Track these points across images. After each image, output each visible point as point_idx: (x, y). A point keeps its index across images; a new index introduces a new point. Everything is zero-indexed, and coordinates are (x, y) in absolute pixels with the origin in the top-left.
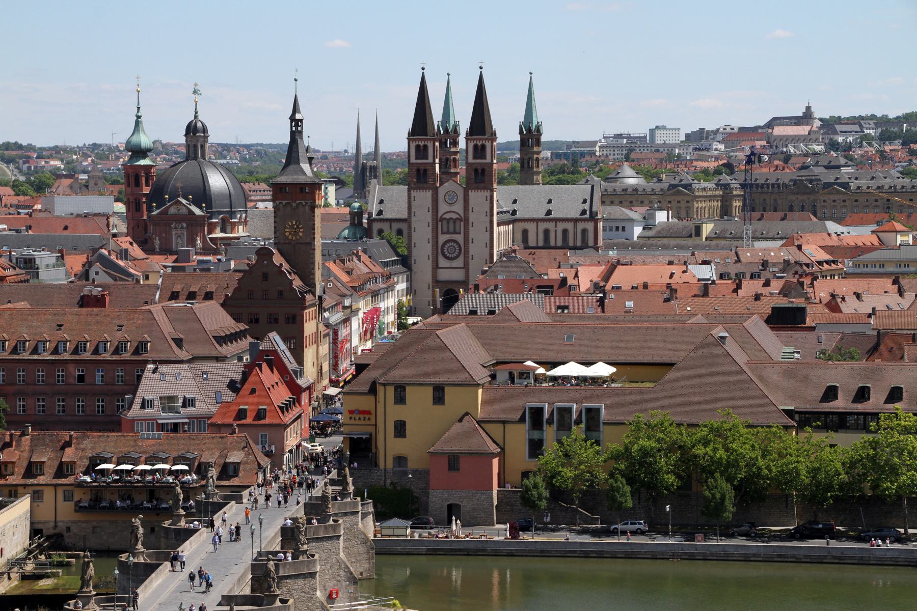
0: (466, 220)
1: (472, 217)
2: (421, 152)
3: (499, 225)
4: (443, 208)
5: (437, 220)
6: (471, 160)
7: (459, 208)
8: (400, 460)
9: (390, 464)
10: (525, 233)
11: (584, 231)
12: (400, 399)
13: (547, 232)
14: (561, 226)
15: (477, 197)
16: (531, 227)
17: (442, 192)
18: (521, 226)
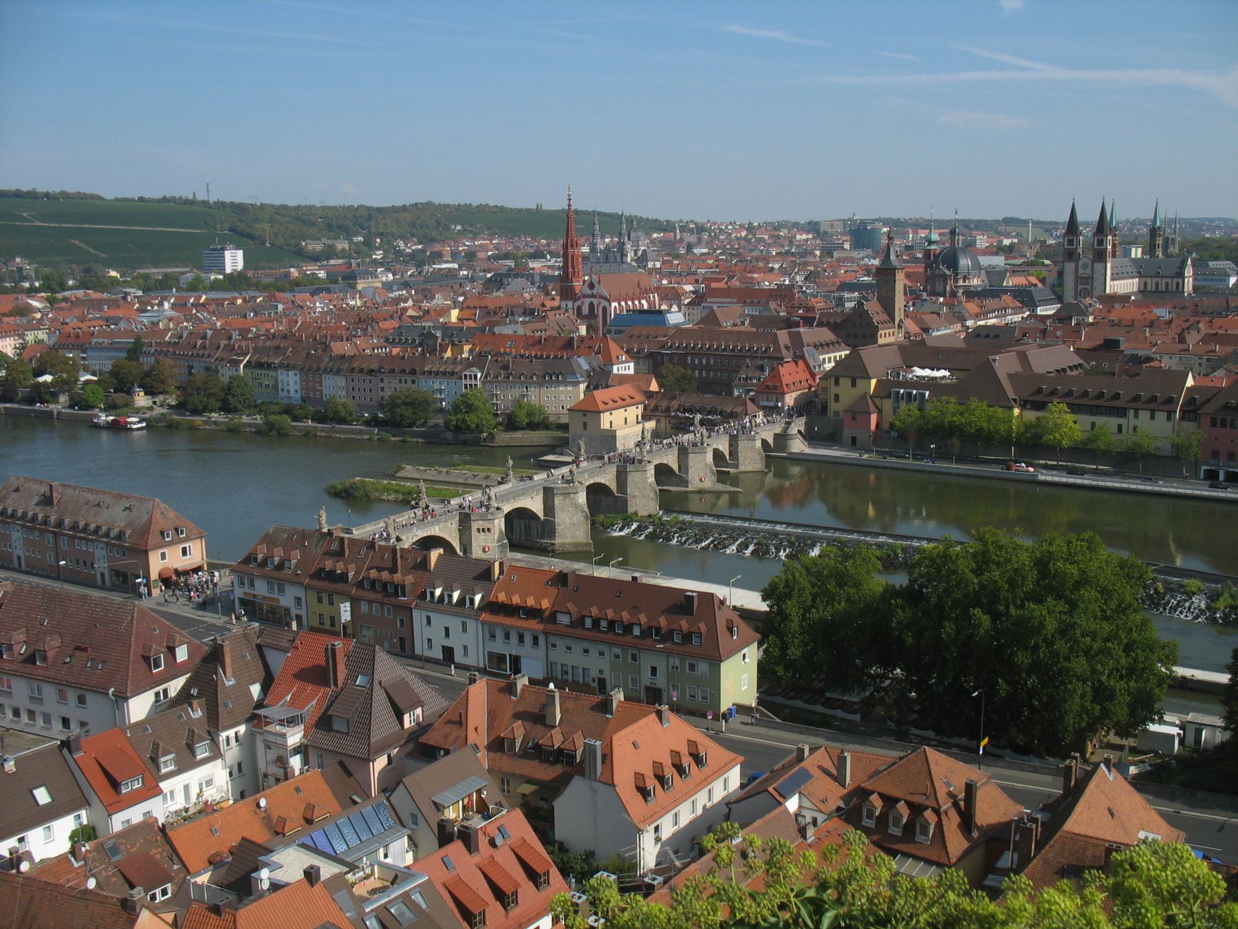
0: (1092, 278)
1: (1095, 276)
2: (1071, 242)
3: (1112, 279)
4: (1081, 271)
5: (1077, 277)
6: (1095, 246)
7: (1088, 271)
8: (836, 413)
9: (832, 414)
10: (1145, 283)
11: (1178, 284)
12: (837, 383)
13: (1157, 284)
14: (1165, 280)
15: (1098, 266)
16: (1149, 280)
17: (1080, 263)
18: (1143, 280)
